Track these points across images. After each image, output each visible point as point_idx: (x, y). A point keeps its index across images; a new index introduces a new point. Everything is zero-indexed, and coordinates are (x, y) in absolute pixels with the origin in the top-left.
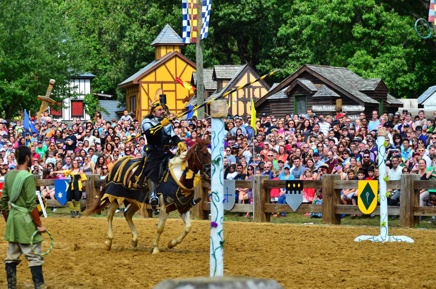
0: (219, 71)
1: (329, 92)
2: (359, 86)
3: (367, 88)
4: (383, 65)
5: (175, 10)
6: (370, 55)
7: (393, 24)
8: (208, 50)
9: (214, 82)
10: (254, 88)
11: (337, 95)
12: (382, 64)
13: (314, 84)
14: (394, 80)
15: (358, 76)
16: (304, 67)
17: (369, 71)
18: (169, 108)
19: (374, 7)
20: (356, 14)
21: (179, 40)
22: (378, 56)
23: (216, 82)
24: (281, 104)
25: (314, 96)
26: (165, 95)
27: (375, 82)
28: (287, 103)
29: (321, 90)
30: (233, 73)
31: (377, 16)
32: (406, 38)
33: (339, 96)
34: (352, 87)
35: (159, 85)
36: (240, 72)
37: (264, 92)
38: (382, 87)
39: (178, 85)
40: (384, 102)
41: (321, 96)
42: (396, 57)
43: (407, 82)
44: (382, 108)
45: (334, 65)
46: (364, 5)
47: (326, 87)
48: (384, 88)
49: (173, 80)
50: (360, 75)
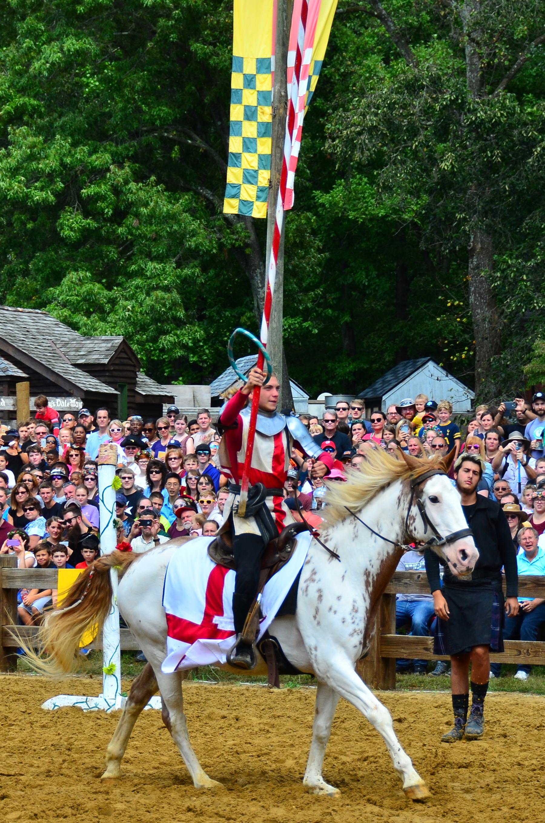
3: (90, 357)
4: (129, 305)
6: (99, 282)
7: (153, 210)
11: (20, 373)
12: (126, 303)
14: (155, 340)
15: (70, 329)
19: (108, 170)
20: (67, 187)
22: (118, 285)
27: (109, 345)
31: (116, 190)
32: (181, 244)
33: (24, 375)
34: (56, 356)
40: (129, 390)
42: (158, 288)
43: (184, 347)
44: (126, 405)
45: (16, 304)
46: (85, 167)
48: (129, 359)
50: (75, 327)
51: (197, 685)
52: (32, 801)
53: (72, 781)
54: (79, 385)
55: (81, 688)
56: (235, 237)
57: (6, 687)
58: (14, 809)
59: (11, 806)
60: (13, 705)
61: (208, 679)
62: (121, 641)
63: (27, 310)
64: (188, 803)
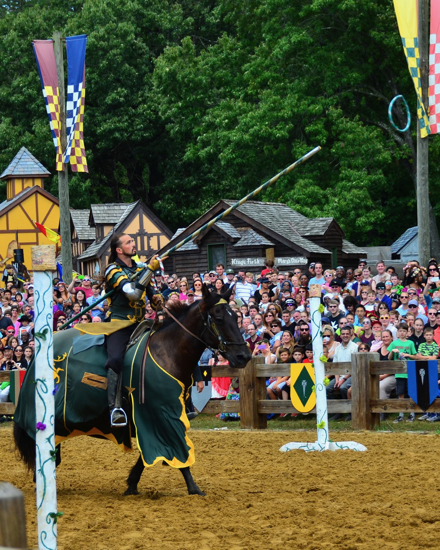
0: (98, 212)
1: (258, 239)
2: (302, 229)
3: (312, 231)
5: (37, 126)
8: (84, 182)
9: (92, 229)
10: (150, 236)
11: (269, 243)
13: (236, 227)
16: (221, 204)
17: (315, 207)
18: (28, 269)
20: (296, 126)
21: (41, 170)
23: (95, 229)
24: (189, 257)
25: (237, 245)
26: (22, 251)
27: (325, 223)
28: (197, 257)
29: (246, 237)
30: (118, 215)
33: (272, 244)
34: (291, 232)
35: (13, 236)
36: (128, 213)
37: (165, 241)
38: (334, 230)
39: (41, 235)
40: (338, 251)
41: (246, 244)
47: (253, 232)
48: (337, 231)
49: (33, 228)
51: (380, 434)
52: (266, 509)
53: (292, 495)
54: (307, 249)
55: (306, 437)
56: (402, 153)
57: (260, 438)
58: (255, 514)
59: (253, 512)
60: (262, 450)
61: (386, 430)
62: (328, 408)
63: (272, 204)
64: (364, 506)
